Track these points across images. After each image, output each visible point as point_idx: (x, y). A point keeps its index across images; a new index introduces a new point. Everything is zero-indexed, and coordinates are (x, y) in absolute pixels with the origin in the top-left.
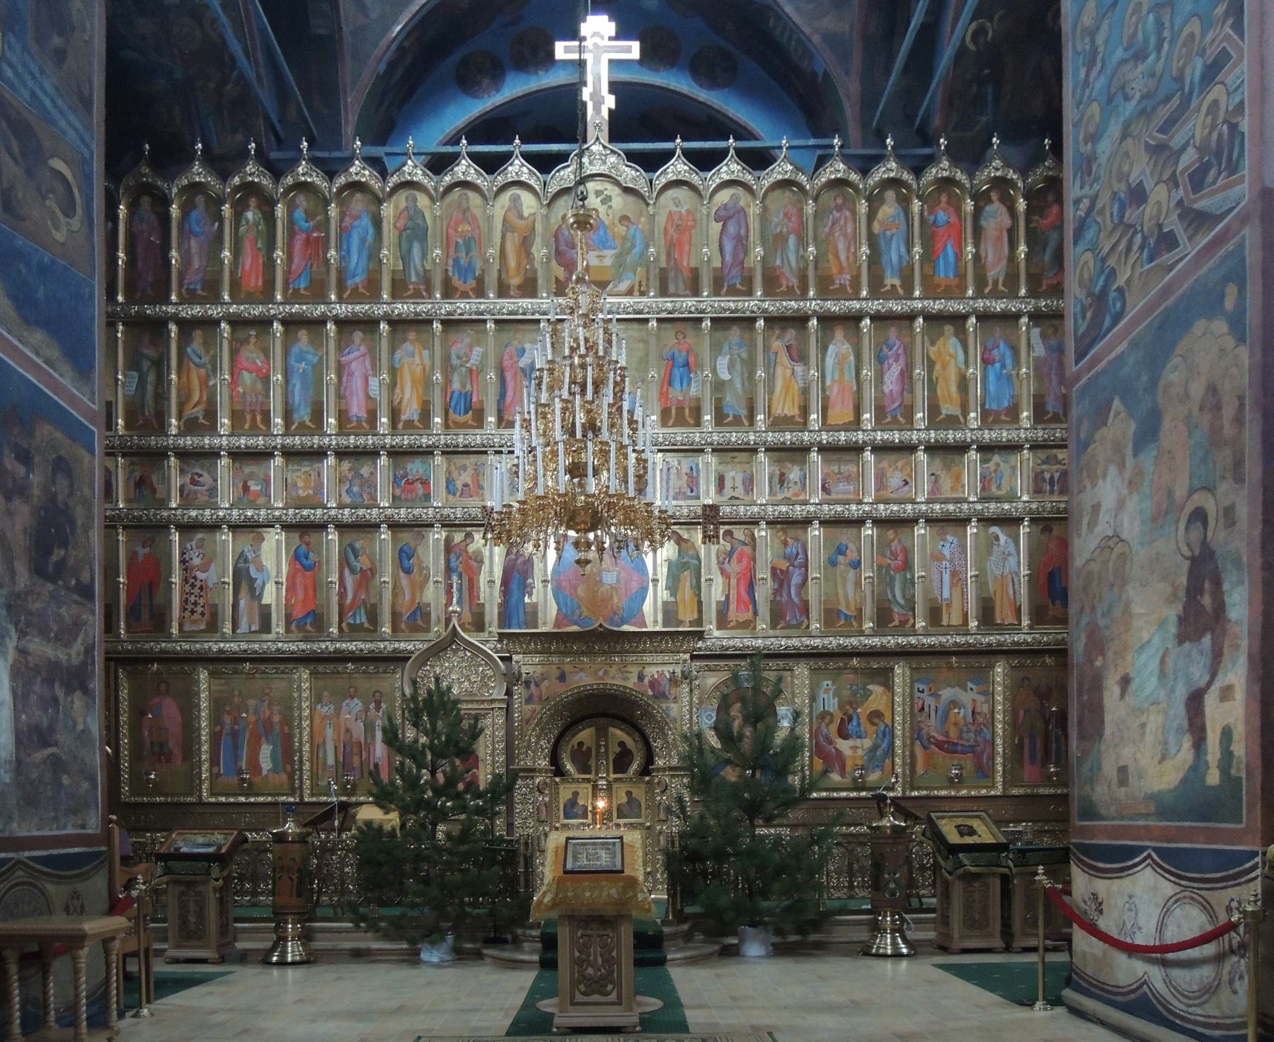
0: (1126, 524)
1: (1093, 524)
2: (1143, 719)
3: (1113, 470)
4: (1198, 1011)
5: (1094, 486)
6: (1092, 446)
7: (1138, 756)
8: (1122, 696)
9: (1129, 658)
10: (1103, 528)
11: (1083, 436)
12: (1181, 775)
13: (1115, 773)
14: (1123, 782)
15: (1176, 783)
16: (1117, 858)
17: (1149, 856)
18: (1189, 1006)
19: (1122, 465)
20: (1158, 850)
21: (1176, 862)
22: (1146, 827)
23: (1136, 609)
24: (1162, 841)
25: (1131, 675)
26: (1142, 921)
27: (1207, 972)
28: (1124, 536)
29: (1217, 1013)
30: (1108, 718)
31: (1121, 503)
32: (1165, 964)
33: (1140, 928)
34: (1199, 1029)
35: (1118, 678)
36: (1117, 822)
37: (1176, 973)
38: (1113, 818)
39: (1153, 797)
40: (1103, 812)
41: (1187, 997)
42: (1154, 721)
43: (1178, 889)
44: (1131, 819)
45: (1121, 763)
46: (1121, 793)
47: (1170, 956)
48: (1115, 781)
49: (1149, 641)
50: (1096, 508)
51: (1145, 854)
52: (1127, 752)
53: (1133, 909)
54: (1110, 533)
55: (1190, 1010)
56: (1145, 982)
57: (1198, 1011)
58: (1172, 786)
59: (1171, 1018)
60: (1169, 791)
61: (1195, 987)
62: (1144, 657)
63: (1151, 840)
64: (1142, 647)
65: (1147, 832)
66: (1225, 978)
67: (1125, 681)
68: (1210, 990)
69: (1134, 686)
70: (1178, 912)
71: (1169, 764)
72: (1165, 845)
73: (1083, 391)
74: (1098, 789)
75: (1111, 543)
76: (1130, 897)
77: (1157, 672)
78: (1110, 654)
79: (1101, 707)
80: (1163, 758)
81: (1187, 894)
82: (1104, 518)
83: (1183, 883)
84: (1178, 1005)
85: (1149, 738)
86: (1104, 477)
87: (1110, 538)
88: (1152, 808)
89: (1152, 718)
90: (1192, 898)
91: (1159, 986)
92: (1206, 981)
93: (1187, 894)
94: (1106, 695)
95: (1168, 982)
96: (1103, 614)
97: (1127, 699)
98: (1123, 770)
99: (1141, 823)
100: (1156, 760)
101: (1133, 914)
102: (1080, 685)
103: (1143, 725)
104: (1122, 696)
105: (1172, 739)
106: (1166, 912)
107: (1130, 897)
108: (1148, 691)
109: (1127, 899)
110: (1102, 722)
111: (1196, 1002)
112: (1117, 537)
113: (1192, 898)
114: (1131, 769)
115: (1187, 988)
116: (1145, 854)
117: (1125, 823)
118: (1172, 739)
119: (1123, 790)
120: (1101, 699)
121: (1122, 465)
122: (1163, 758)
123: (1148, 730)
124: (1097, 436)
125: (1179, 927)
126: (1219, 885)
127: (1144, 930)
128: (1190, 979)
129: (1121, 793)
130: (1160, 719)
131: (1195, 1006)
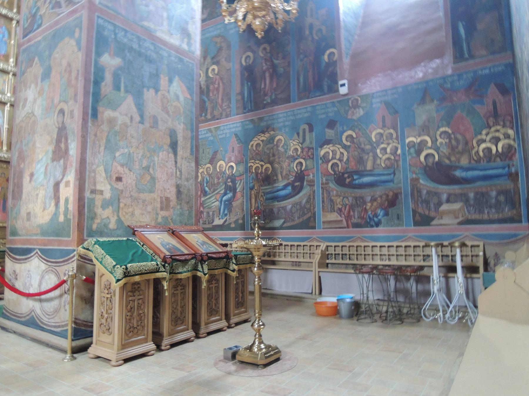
0: (36, 109)
1: (24, 106)
2: (38, 192)
3: (33, 86)
4: (53, 321)
5: (25, 91)
6: (26, 74)
7: (35, 208)
8: (30, 181)
9: (34, 165)
10: (28, 108)
11: (23, 69)
12: (50, 217)
13: (25, 215)
14: (29, 219)
15: (48, 220)
16: (24, 253)
17: (37, 252)
18: (49, 319)
19: (37, 84)
20: (39, 249)
21: (47, 255)
22: (36, 240)
23: (38, 145)
24: (41, 245)
25: (35, 173)
26: (33, 282)
27: (56, 303)
28: (36, 113)
29: (59, 321)
30: (24, 191)
31: (35, 100)
32: (41, 301)
33: (32, 285)
34: (53, 329)
35: (29, 173)
36: (25, 238)
37: (45, 305)
38: (24, 236)
39: (40, 226)
40: (20, 232)
41: (49, 315)
42: (42, 193)
43: (47, 266)
44: (30, 236)
45: (28, 211)
46: (27, 224)
47: (43, 297)
48: (25, 219)
49: (42, 159)
50: (26, 100)
51: (35, 252)
52: (31, 206)
53: (30, 276)
54: (30, 111)
55: (50, 321)
56: (33, 311)
57: (53, 321)
58: (47, 222)
59: (42, 325)
60: (46, 224)
61: (52, 310)
62: (39, 166)
63: (38, 245)
64: (39, 161)
65: (37, 242)
66: (63, 304)
67: (32, 175)
68: (57, 311)
69: (35, 177)
70: (47, 277)
71: (46, 212)
72: (43, 247)
73: (25, 50)
74: (18, 222)
75: (30, 116)
76: (29, 271)
77: (44, 172)
78: (27, 162)
79: (22, 186)
80: (44, 209)
81: (50, 269)
82: (28, 105)
83: (49, 264)
84: (45, 319)
85: (39, 201)
86: (30, 87)
87: (30, 114)
88: (39, 232)
89: (41, 191)
90: (52, 271)
91: (38, 311)
92: (56, 307)
93: (50, 269)
94: (24, 180)
95: (42, 309)
96: (25, 145)
97: (32, 183)
98: (29, 214)
99: (35, 238)
100: (41, 210)
101: (29, 279)
102: (14, 175)
103: (37, 195)
104: (30, 181)
105: (47, 201)
106: (42, 277)
107: (29, 271)
108: (40, 180)
109: (27, 272)
110: (22, 192)
111: (52, 317)
112: (33, 113)
113: (52, 271)
114: (32, 214)
115: (48, 311)
116: (35, 252)
117: (28, 238)
118: (47, 201)
119: (28, 223)
120: (22, 182)
121: (37, 84)
122: (44, 209)
123: (39, 197)
124: (28, 70)
125: (47, 284)
126: (63, 264)
127: (33, 286)
128: (49, 306)
129: (27, 224)
130: (44, 192)
131: (52, 318)
